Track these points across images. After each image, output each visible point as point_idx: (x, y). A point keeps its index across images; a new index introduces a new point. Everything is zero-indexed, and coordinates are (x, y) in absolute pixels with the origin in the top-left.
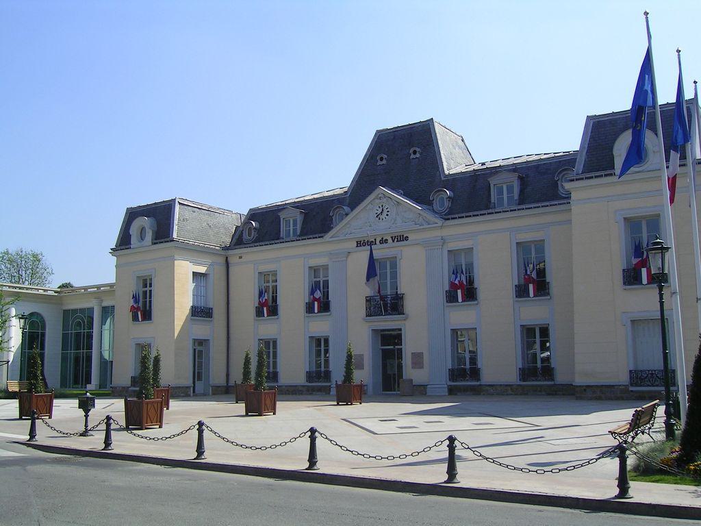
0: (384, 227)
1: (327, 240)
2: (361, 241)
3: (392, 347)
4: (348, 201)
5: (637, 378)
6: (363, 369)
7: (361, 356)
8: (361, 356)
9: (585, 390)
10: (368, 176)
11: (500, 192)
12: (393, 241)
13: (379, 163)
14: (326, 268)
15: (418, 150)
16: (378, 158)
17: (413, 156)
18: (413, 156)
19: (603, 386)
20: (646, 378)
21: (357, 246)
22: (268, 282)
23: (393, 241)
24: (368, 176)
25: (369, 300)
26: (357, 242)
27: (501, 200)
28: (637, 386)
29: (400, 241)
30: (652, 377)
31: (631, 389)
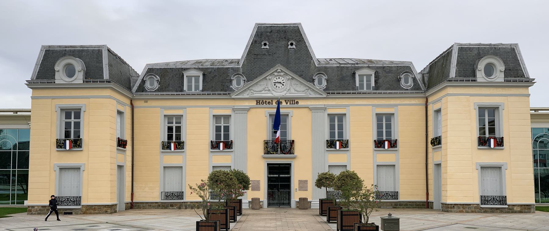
0: (279, 93)
1: (233, 97)
2: (260, 101)
3: (277, 176)
4: (241, 70)
5: (485, 200)
6: (260, 190)
7: (258, 182)
8: (258, 182)
9: (454, 207)
10: (255, 55)
11: (361, 81)
12: (287, 103)
13: (263, 47)
14: (227, 117)
15: (294, 43)
16: (263, 43)
17: (290, 47)
18: (290, 47)
19: (464, 204)
20: (490, 200)
21: (257, 104)
22: (172, 123)
23: (287, 103)
24: (255, 55)
25: (266, 143)
26: (257, 101)
27: (362, 86)
28: (485, 204)
29: (292, 104)
30: (494, 200)
31: (482, 206)
